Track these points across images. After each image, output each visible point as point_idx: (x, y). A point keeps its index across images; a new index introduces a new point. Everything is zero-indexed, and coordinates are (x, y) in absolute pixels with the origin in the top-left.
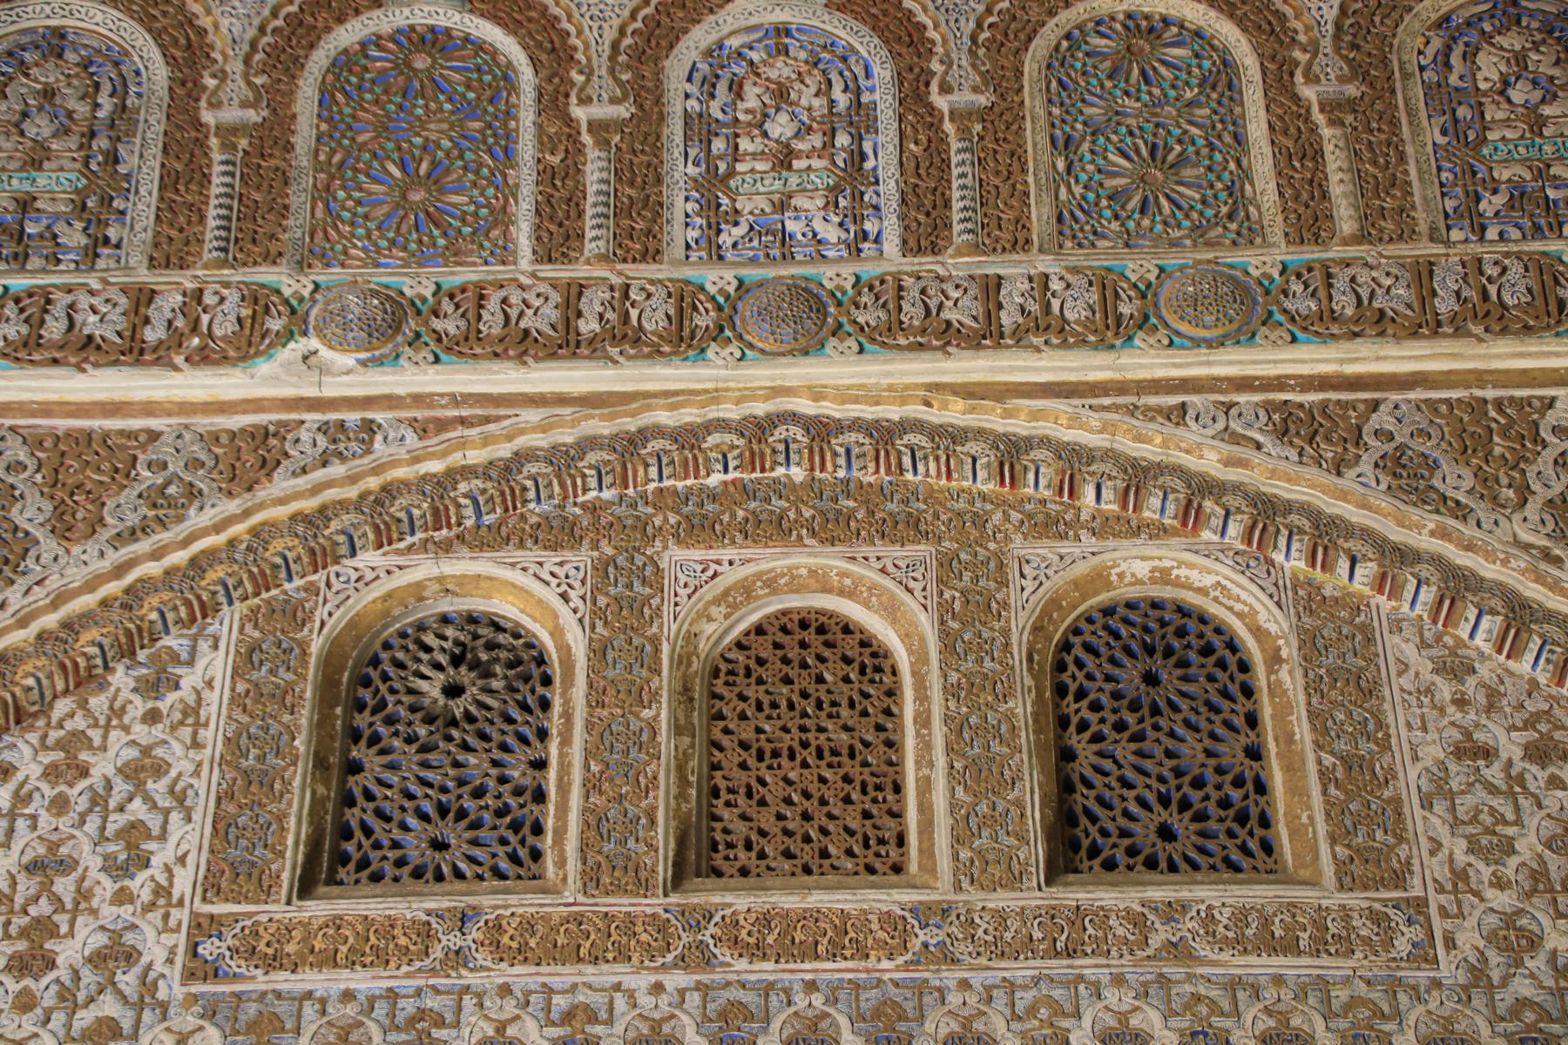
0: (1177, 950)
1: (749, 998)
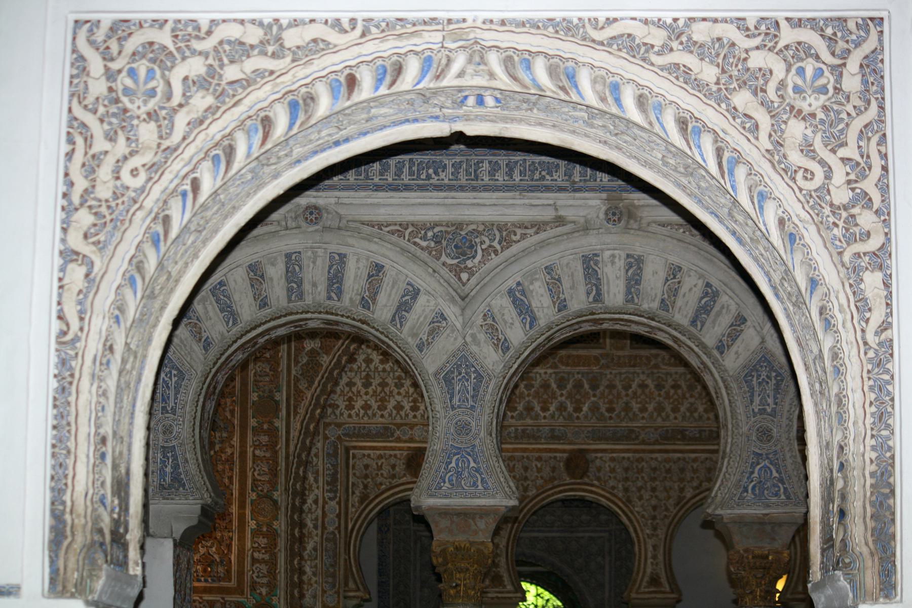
0: (656, 366)
1: (566, 376)
